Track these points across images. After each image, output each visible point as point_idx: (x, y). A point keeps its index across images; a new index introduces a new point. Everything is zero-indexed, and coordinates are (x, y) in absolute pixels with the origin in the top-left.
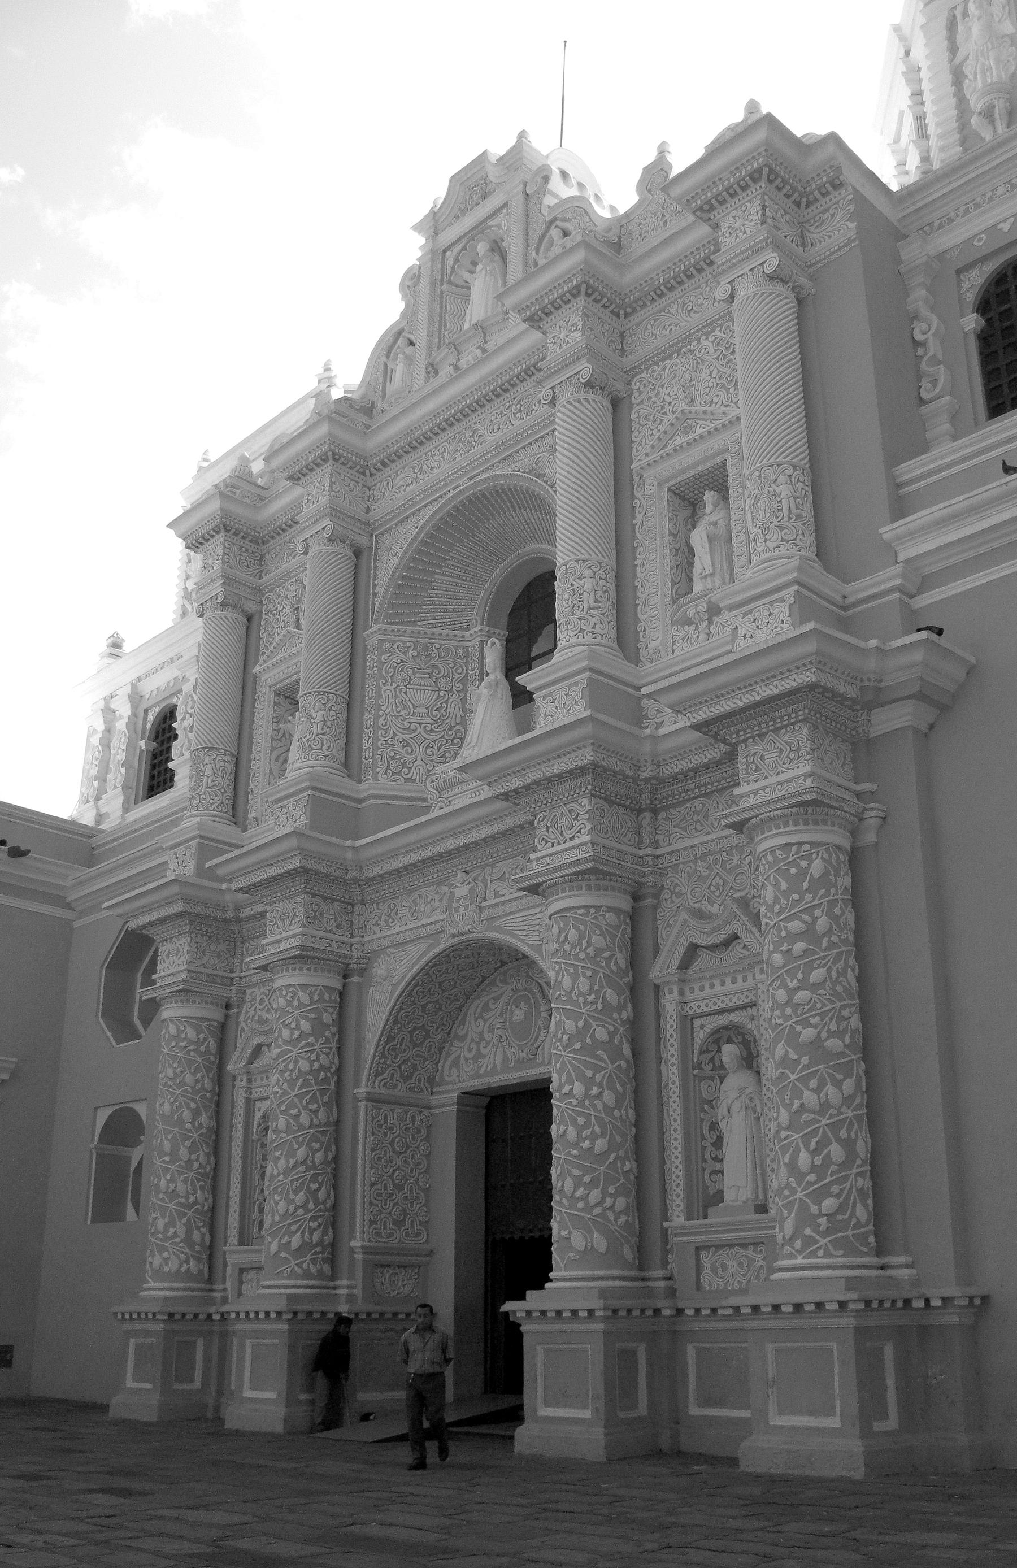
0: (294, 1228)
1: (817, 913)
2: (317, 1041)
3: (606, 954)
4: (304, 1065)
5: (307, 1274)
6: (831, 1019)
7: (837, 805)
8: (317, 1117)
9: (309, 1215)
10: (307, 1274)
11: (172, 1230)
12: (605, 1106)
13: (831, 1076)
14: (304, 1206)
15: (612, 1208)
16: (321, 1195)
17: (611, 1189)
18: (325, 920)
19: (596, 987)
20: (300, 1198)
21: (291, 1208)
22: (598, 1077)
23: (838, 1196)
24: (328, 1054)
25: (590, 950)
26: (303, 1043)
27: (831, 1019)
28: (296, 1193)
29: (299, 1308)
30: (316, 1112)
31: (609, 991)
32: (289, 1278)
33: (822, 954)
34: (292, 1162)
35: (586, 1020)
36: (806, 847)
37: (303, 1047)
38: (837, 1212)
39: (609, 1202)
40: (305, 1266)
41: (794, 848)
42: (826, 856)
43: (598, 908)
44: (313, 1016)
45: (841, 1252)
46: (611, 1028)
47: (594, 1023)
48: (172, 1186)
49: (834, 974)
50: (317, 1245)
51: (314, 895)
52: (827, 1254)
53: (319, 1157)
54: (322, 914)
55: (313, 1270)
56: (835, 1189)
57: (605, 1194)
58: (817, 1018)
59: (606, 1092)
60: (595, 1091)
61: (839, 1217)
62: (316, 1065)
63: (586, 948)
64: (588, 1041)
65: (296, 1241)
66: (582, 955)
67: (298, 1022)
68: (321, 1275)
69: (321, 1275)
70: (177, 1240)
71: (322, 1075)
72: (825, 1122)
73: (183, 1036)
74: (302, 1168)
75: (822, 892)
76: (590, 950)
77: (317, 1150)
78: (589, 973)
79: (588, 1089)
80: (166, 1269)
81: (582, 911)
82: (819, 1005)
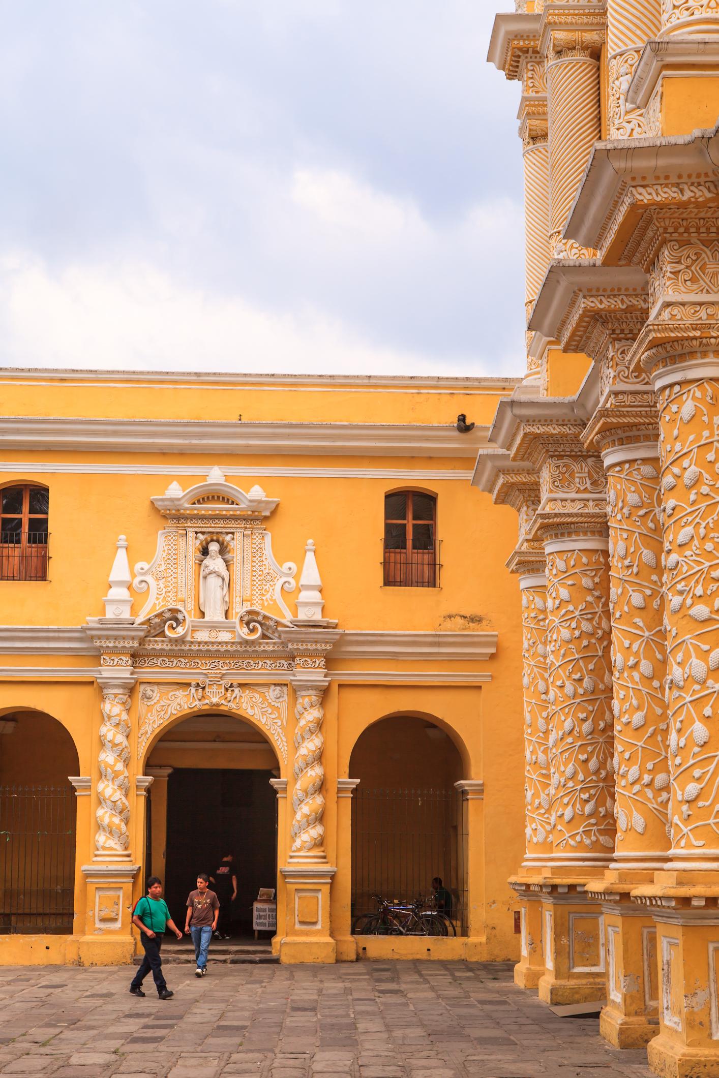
0: (566, 800)
1: (686, 463)
2: (576, 608)
3: (642, 512)
4: (565, 634)
5: (580, 846)
6: (697, 582)
7: (698, 334)
8: (581, 686)
9: (579, 787)
10: (580, 846)
11: (537, 802)
12: (642, 676)
13: (697, 648)
14: (573, 777)
15: (649, 785)
16: (593, 764)
17: (650, 766)
18: (577, 480)
19: (632, 550)
20: (569, 770)
21: (562, 781)
22: (635, 647)
23: (699, 779)
24: (590, 620)
25: (625, 511)
26: (563, 611)
27: (697, 582)
28: (566, 766)
29: (557, 881)
30: (580, 680)
31: (645, 551)
32: (564, 851)
33: (689, 510)
34: (560, 733)
35: (624, 588)
36: (677, 388)
37: (563, 616)
38: (697, 798)
39: (647, 778)
40: (578, 838)
41: (667, 392)
42: (698, 394)
43: (632, 462)
44: (570, 582)
45: (701, 843)
46: (648, 592)
47: (630, 589)
48: (534, 758)
49: (702, 531)
50: (590, 816)
51: (560, 457)
52: (689, 845)
53: (586, 727)
54: (572, 475)
55: (587, 842)
56: (697, 773)
57: (642, 770)
58: (683, 583)
59: (643, 662)
60: (631, 662)
61: (701, 804)
62: (577, 633)
63: (622, 509)
64: (626, 609)
65: (568, 813)
66: (619, 517)
67: (557, 590)
68: (595, 846)
69: (595, 846)
70: (542, 811)
71: (585, 643)
72: (688, 699)
73: (533, 607)
74: (570, 740)
75: (692, 437)
76: (625, 511)
77: (584, 720)
78: (625, 535)
79: (626, 660)
80: (535, 840)
81: (618, 469)
82: (685, 568)
